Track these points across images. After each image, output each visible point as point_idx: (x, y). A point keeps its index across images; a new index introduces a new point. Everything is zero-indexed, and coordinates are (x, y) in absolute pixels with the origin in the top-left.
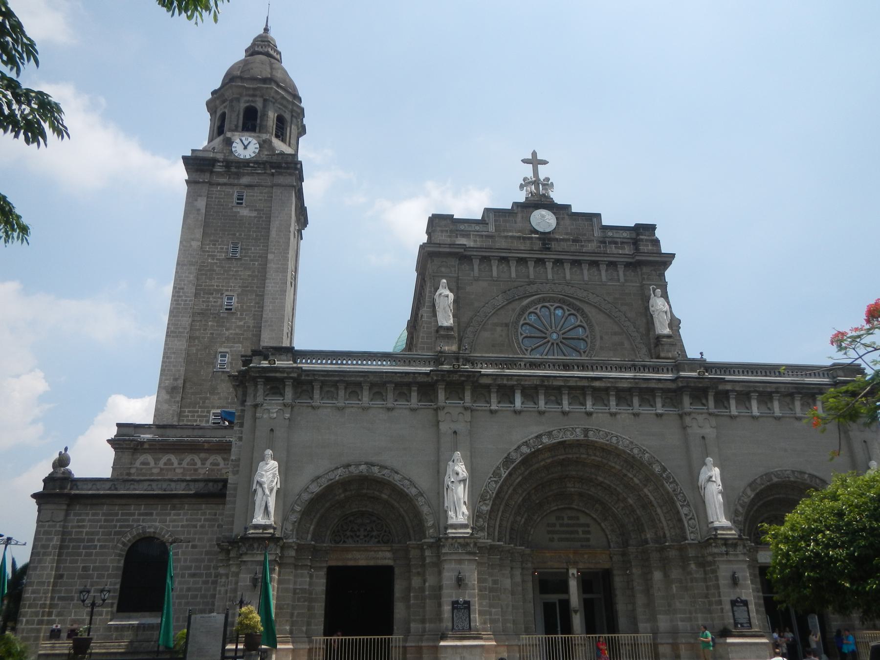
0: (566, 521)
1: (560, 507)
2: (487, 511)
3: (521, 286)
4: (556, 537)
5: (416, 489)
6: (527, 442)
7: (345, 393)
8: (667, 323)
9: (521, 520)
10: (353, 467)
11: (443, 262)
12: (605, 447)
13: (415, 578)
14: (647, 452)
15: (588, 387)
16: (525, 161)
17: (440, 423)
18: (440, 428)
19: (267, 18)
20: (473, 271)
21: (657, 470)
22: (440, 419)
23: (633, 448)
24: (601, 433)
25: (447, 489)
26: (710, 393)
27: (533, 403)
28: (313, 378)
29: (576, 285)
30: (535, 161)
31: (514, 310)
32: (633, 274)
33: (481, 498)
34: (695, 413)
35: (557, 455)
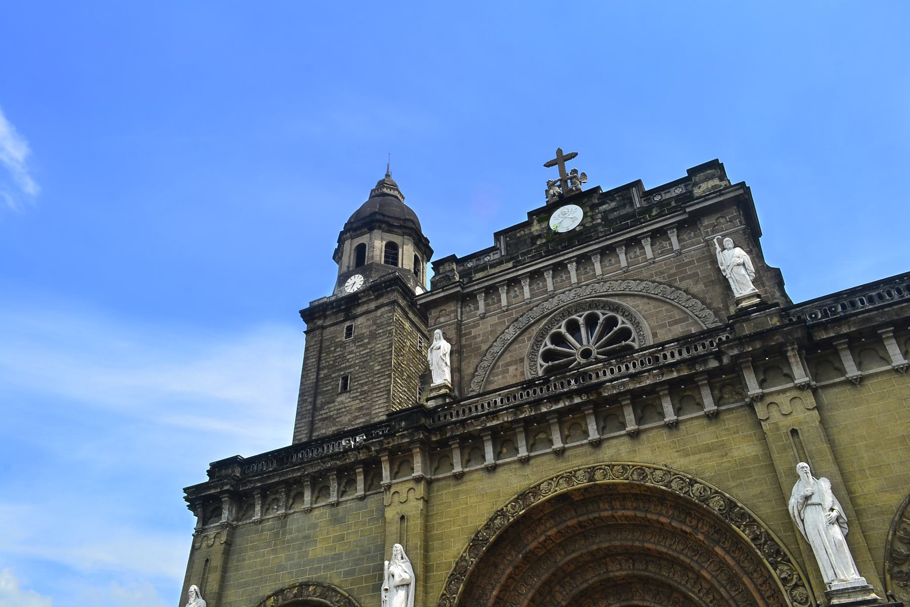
3: (537, 306)
6: (502, 509)
7: (288, 496)
8: (752, 278)
11: (442, 310)
12: (634, 491)
14: (696, 482)
16: (548, 165)
19: (388, 165)
20: (478, 309)
21: (716, 509)
23: (671, 482)
24: (615, 467)
26: (789, 354)
28: (250, 487)
29: (612, 278)
30: (561, 159)
31: (529, 339)
32: (692, 234)
34: (771, 393)
35: (565, 521)
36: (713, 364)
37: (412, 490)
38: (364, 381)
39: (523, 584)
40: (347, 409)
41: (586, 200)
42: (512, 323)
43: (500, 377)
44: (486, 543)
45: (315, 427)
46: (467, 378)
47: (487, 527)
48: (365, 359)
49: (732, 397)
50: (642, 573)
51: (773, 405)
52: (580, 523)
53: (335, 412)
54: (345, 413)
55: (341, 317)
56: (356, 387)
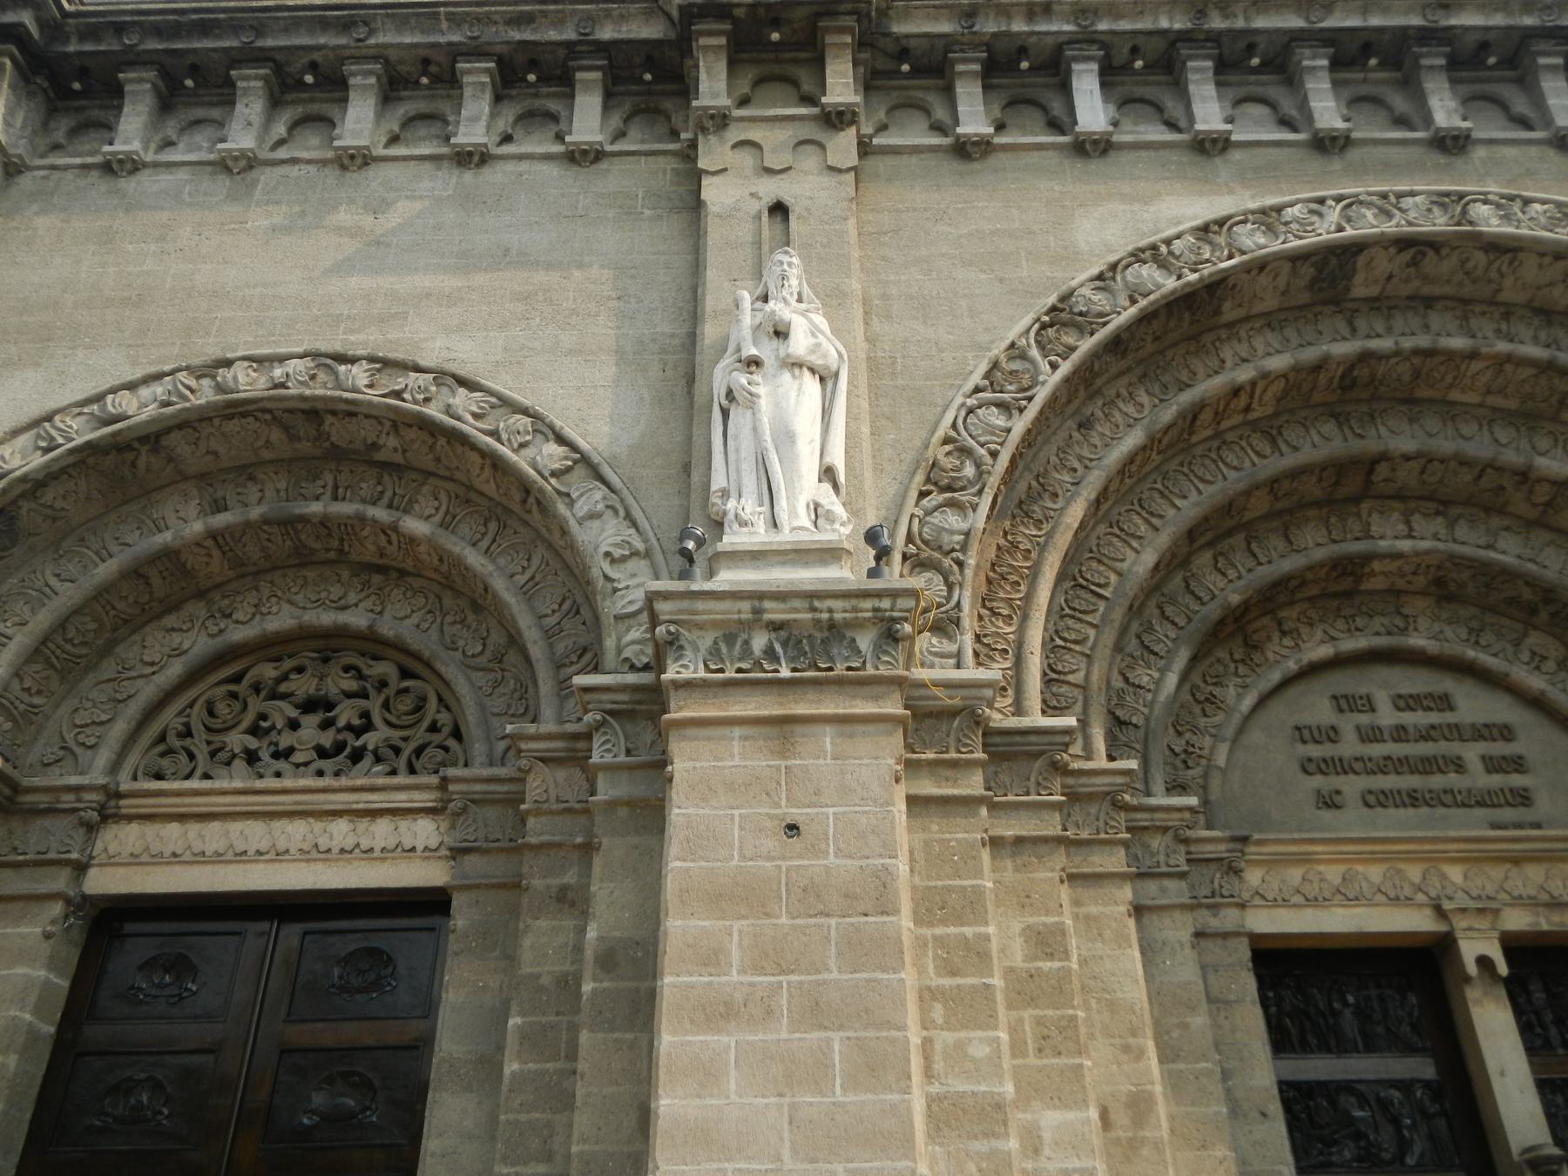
0: (1387, 716)
1: (1350, 644)
2: (967, 534)
4: (1351, 786)
5: (561, 450)
6: (1154, 247)
9: (1158, 683)
10: (239, 367)
13: (543, 923)
15: (1428, 36)
17: (706, 181)
18: (704, 196)
22: (701, 164)
25: (725, 414)
27: (1163, 128)
28: (116, 47)
33: (928, 480)
37: (810, 148)
39: (1139, 510)
44: (1105, 324)
50: (1482, 553)
52: (1365, 357)
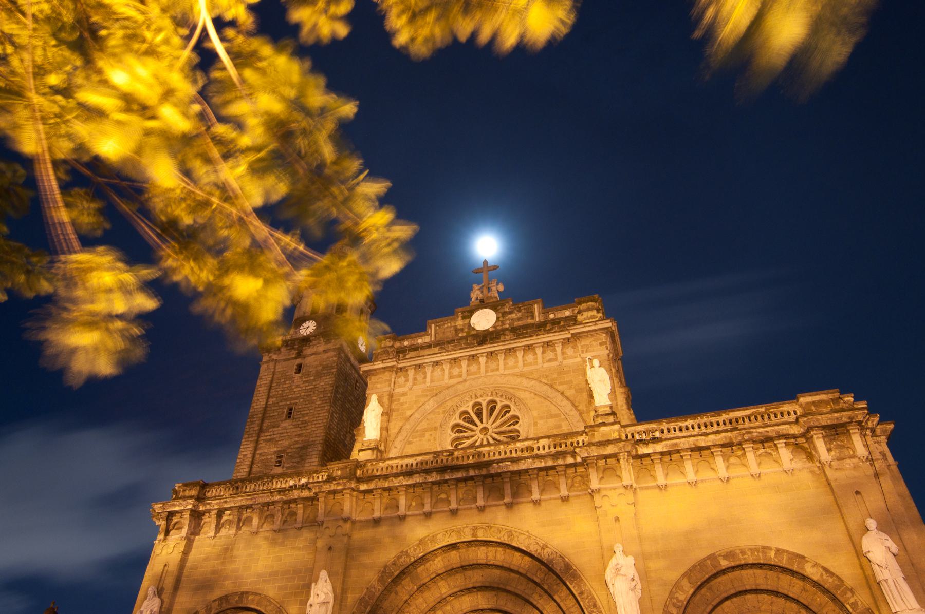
14: (547, 547)
34: (606, 489)
36: (570, 460)
38: (305, 412)
40: (289, 434)
41: (500, 307)
42: (433, 397)
43: (417, 439)
45: (260, 445)
46: (392, 437)
47: (394, 564)
48: (309, 393)
49: (580, 486)
51: (606, 498)
53: (278, 436)
54: (286, 438)
55: (293, 353)
56: (298, 416)
